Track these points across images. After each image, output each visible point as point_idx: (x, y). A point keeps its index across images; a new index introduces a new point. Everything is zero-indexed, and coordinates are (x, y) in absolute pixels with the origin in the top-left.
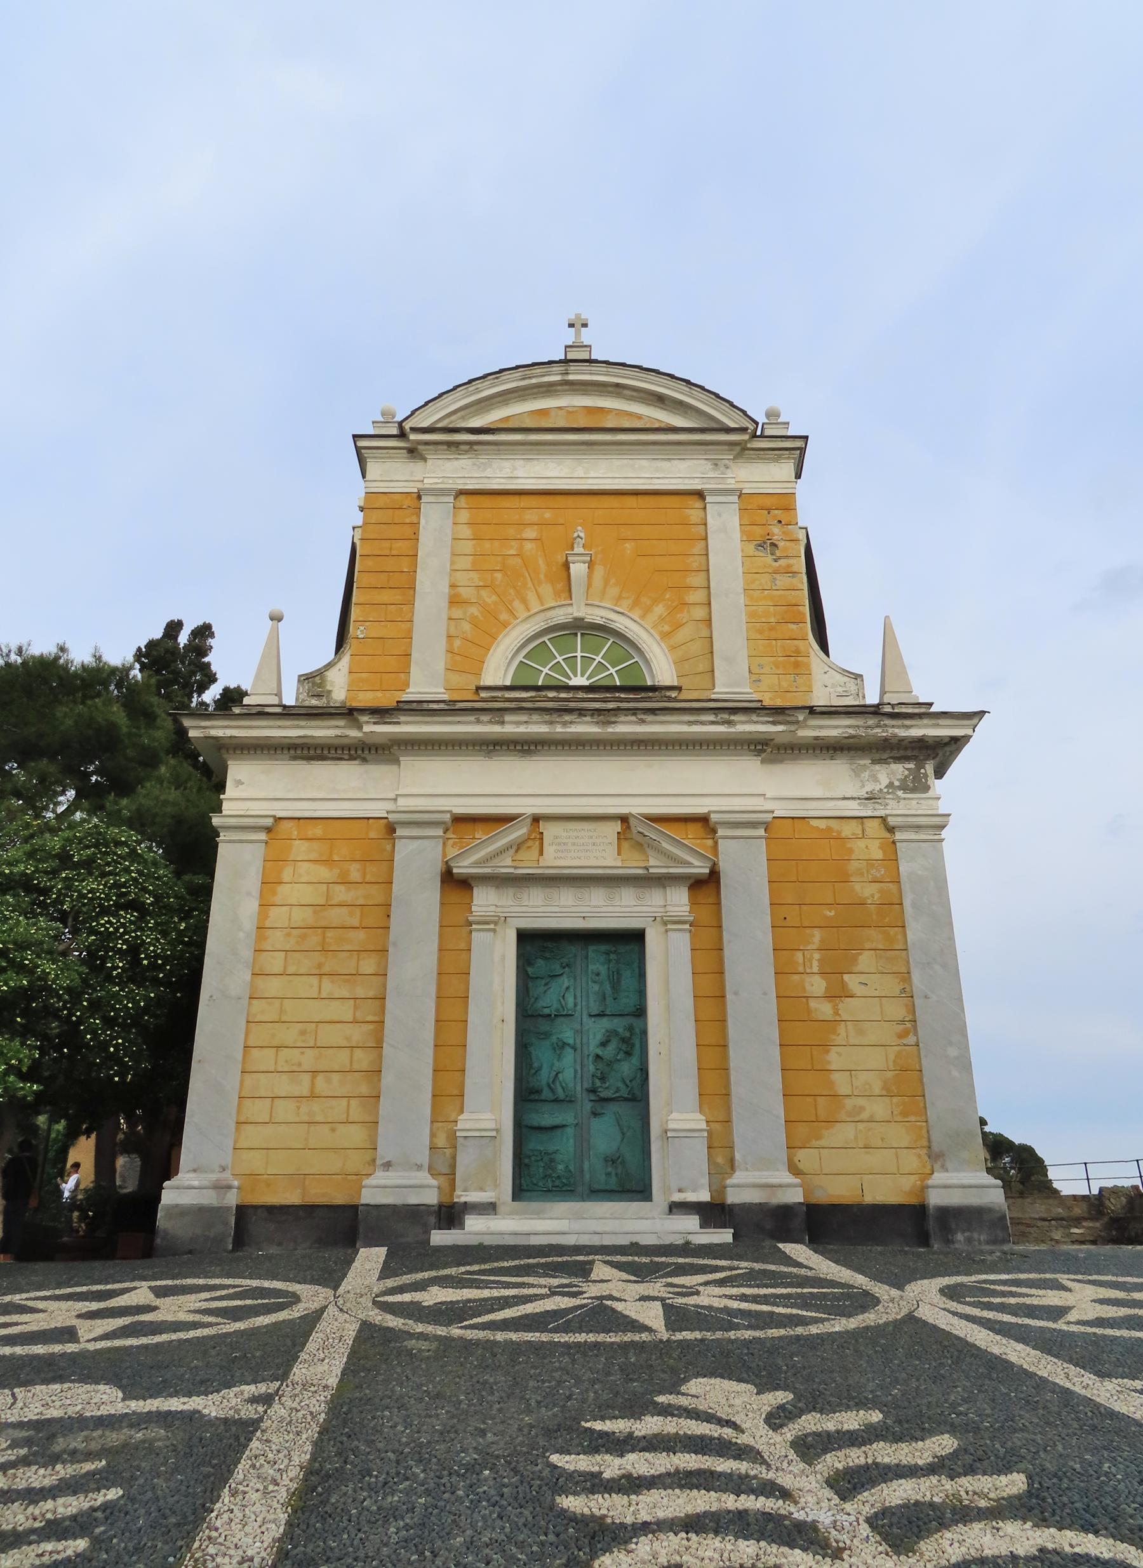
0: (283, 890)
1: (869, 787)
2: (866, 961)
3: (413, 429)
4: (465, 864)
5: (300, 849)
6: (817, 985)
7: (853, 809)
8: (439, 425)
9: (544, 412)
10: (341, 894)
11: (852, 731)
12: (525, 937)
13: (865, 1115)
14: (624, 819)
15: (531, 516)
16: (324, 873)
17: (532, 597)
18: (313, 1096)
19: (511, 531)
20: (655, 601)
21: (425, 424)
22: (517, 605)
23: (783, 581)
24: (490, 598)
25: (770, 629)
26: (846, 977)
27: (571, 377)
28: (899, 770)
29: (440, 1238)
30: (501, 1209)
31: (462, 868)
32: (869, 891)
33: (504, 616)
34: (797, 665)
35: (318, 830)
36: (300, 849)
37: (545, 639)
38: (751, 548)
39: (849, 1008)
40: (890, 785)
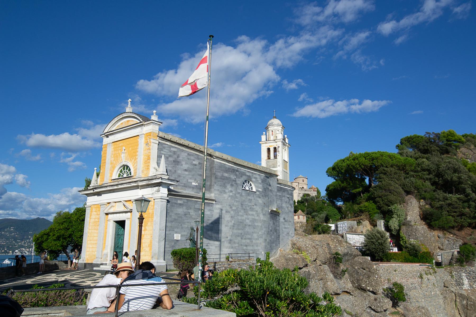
0: (92, 216)
1: (153, 192)
4: (105, 211)
5: (94, 210)
7: (150, 196)
8: (109, 131)
9: (122, 123)
11: (146, 183)
13: (145, 250)
18: (93, 248)
20: (133, 159)
21: (106, 132)
25: (146, 162)
26: (146, 227)
27: (124, 116)
28: (157, 188)
29: (95, 269)
30: (107, 264)
35: (95, 207)
37: (122, 168)
38: (145, 145)
40: (155, 191)
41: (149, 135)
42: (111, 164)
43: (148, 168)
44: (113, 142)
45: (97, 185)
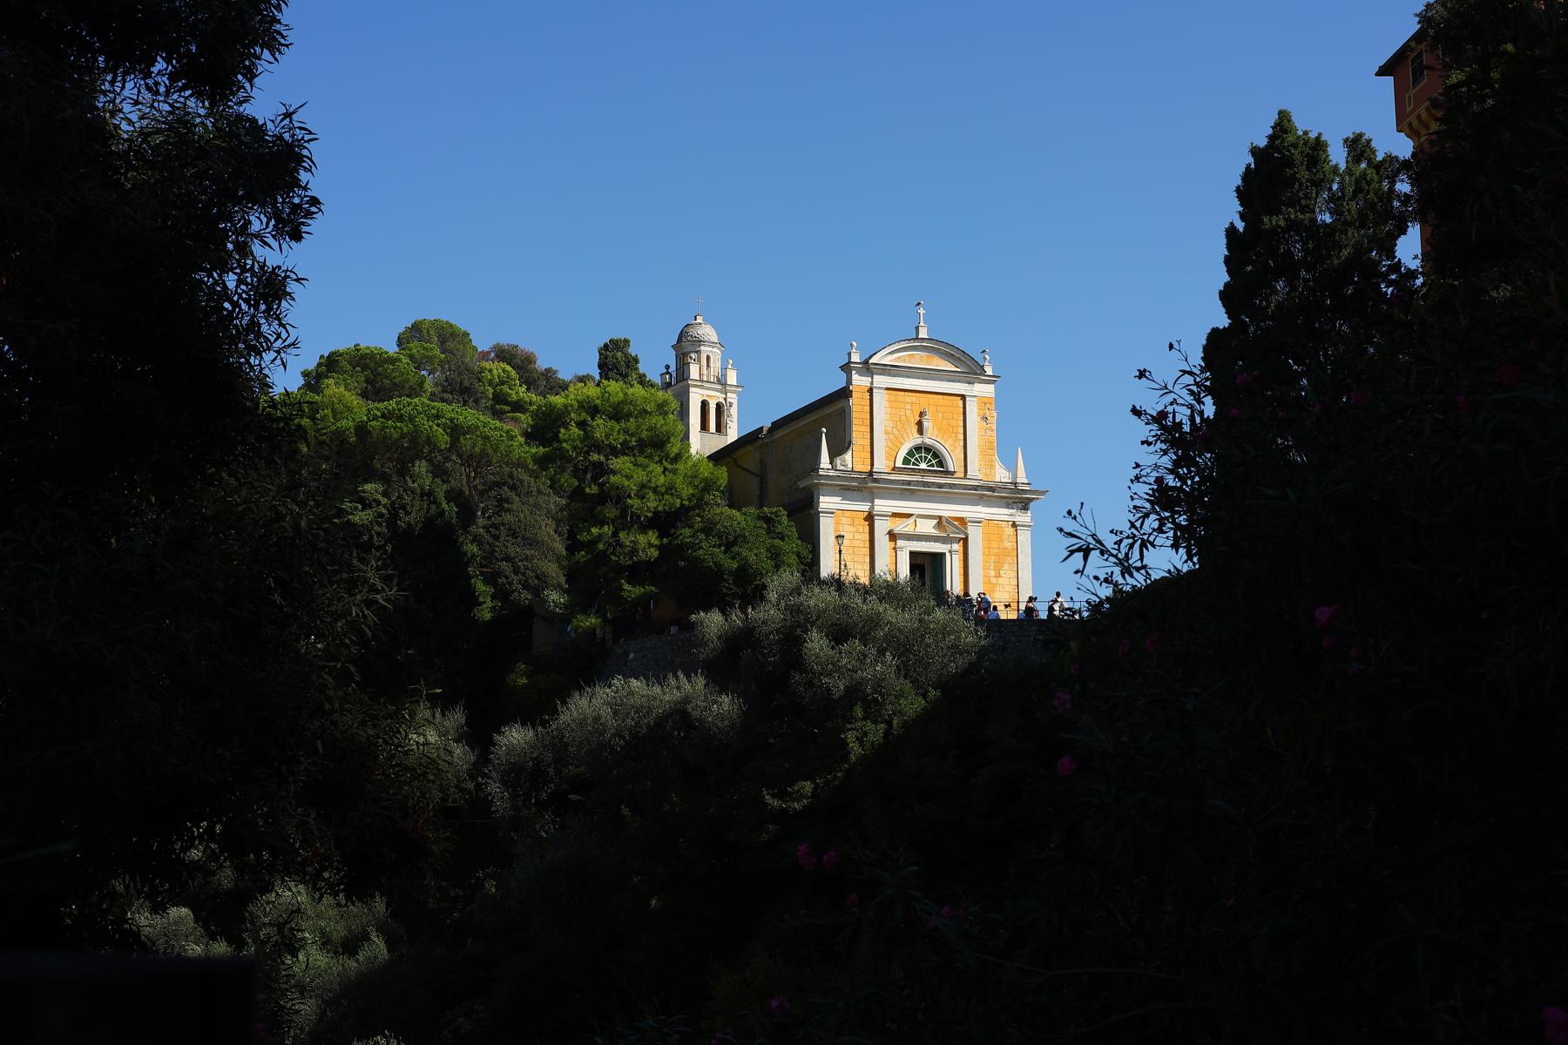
2: (1006, 567)
3: (872, 364)
6: (992, 573)
10: (857, 536)
12: (911, 553)
14: (940, 518)
15: (908, 400)
16: (852, 529)
17: (909, 431)
19: (902, 405)
20: (949, 438)
22: (905, 436)
23: (989, 433)
24: (896, 433)
31: (897, 530)
32: (1008, 545)
33: (901, 440)
34: (992, 465)
35: (848, 514)
36: (844, 520)
39: (1000, 581)
41: (984, 402)
42: (887, 433)
43: (992, 467)
44: (887, 389)
45: (842, 468)
